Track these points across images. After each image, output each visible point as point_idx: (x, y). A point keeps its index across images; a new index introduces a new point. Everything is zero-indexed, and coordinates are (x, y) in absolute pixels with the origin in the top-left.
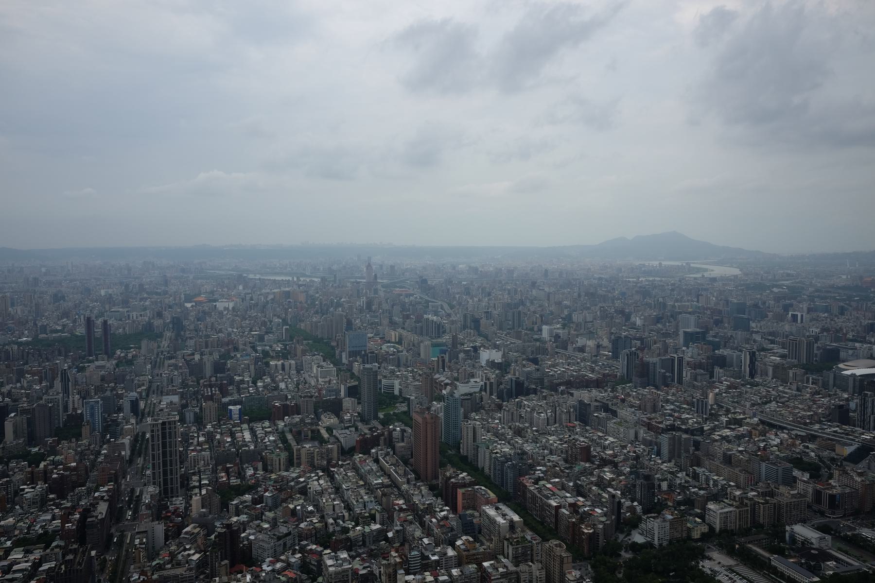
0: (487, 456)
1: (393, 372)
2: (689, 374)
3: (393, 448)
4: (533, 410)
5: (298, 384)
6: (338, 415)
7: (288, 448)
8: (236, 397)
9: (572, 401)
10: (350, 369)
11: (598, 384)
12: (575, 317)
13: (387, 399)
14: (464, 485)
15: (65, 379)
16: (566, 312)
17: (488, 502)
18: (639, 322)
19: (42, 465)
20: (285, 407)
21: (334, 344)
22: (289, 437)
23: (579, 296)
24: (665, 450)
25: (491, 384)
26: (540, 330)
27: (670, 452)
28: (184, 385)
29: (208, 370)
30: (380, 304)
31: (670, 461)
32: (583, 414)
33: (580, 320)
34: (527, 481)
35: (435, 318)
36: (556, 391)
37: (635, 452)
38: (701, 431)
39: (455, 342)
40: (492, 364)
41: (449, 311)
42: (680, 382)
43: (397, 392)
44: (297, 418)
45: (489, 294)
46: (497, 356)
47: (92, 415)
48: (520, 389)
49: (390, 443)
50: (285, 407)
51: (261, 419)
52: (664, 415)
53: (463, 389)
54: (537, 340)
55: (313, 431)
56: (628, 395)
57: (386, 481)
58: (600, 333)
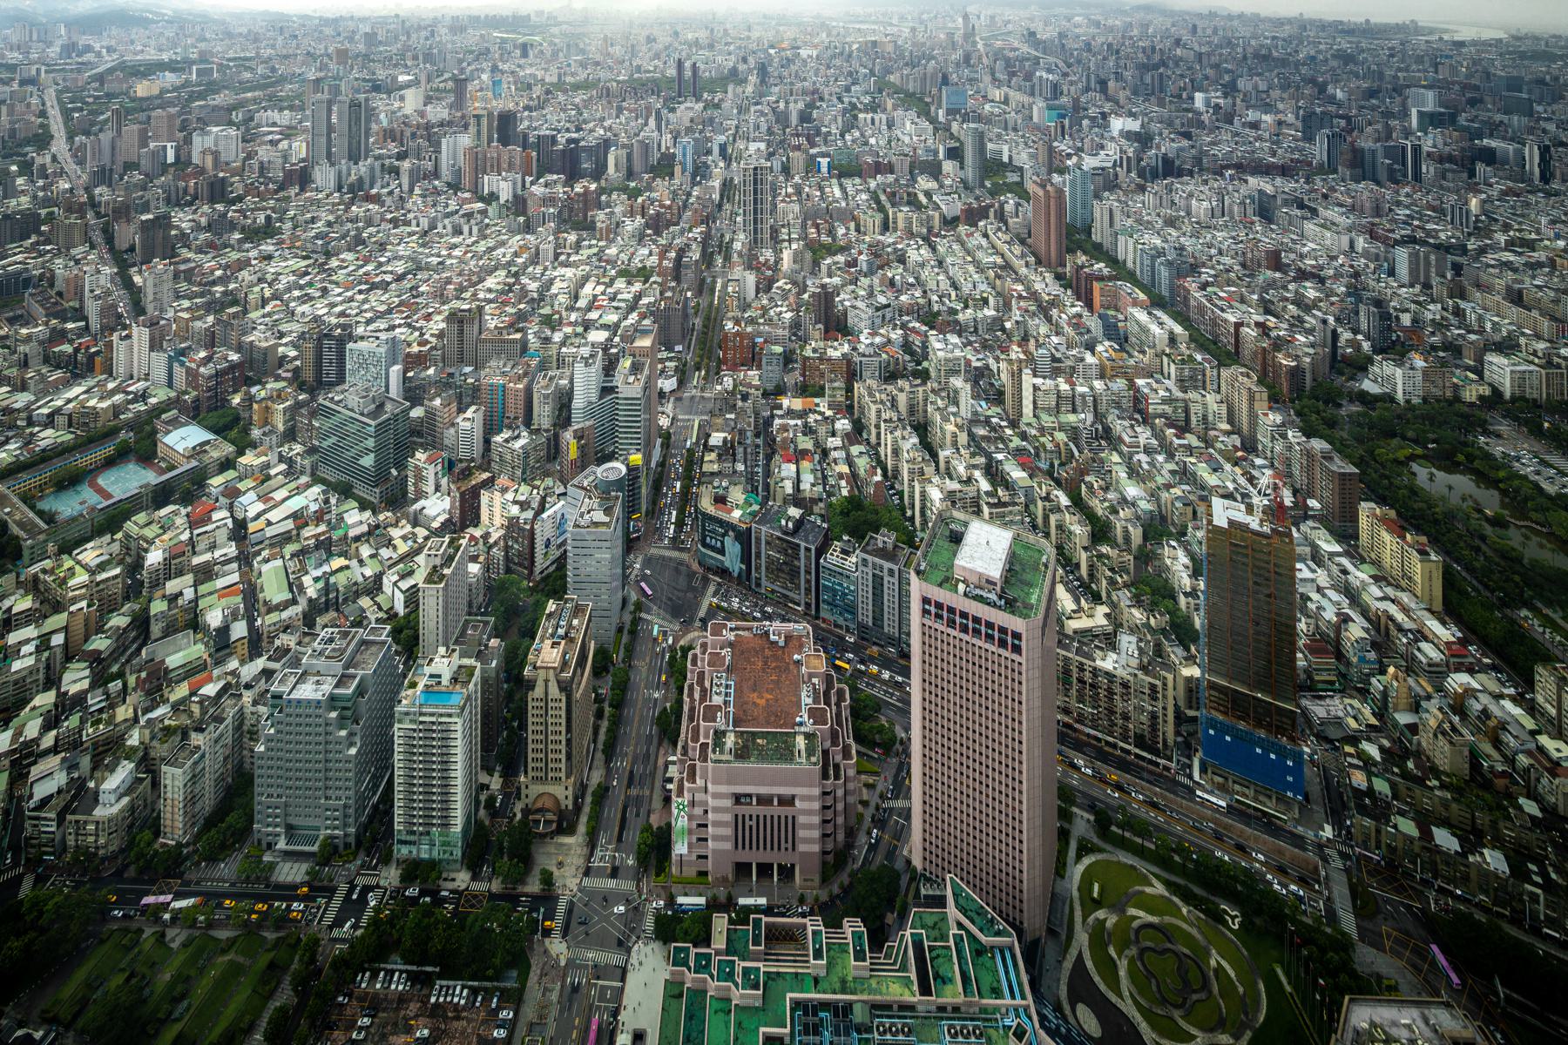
0: (1131, 248)
1: (999, 136)
2: (1432, 170)
3: (1006, 224)
4: (1191, 195)
5: (889, 142)
6: (937, 179)
7: (881, 209)
8: (824, 149)
9: (1243, 190)
10: (948, 129)
11: (1285, 171)
12: (1241, 83)
13: (992, 168)
14: (1101, 279)
15: (659, 119)
16: (1227, 78)
17: (1135, 303)
18: (1340, 94)
19: (640, 200)
20: (877, 164)
21: (928, 100)
22: (883, 198)
23: (1245, 57)
24: (1403, 270)
25: (1129, 158)
26: (1192, 98)
27: (1411, 273)
28: (770, 131)
29: (794, 120)
30: (980, 58)
31: (1412, 286)
32: (1265, 210)
33: (1249, 88)
34: (1191, 284)
35: (1050, 77)
36: (1222, 175)
37: (1352, 266)
38: (1464, 250)
39: (1077, 107)
40: (1128, 135)
41: (1066, 70)
42: (1417, 176)
43: (1005, 159)
44: (891, 178)
45: (1118, 52)
46: (1134, 125)
47: (684, 155)
48: (1170, 168)
49: (1001, 217)
50: (877, 164)
51: (850, 175)
52: (1396, 221)
53: (1090, 162)
54: (1188, 110)
55: (909, 194)
56: (1333, 189)
57: (999, 260)
58: (1281, 106)
